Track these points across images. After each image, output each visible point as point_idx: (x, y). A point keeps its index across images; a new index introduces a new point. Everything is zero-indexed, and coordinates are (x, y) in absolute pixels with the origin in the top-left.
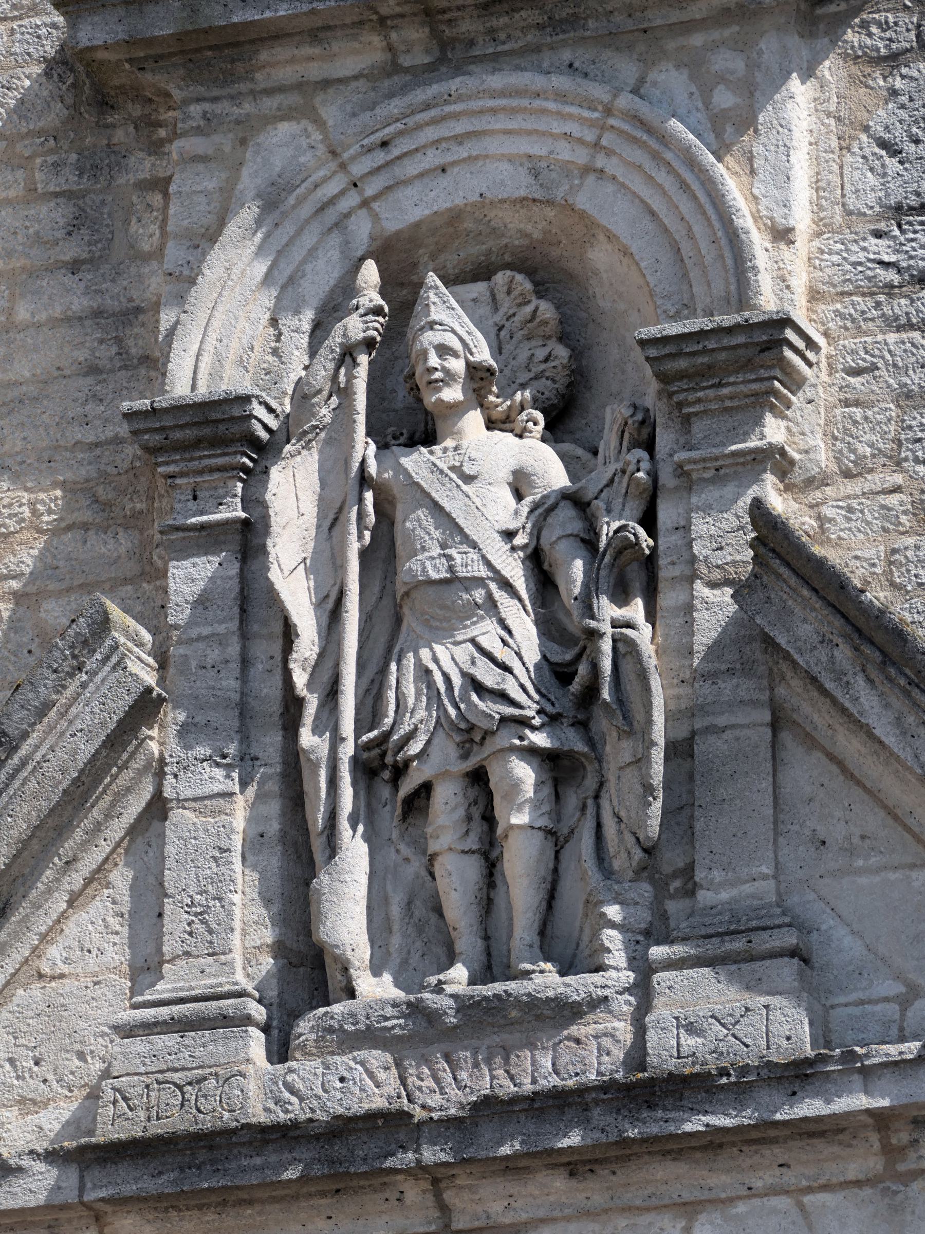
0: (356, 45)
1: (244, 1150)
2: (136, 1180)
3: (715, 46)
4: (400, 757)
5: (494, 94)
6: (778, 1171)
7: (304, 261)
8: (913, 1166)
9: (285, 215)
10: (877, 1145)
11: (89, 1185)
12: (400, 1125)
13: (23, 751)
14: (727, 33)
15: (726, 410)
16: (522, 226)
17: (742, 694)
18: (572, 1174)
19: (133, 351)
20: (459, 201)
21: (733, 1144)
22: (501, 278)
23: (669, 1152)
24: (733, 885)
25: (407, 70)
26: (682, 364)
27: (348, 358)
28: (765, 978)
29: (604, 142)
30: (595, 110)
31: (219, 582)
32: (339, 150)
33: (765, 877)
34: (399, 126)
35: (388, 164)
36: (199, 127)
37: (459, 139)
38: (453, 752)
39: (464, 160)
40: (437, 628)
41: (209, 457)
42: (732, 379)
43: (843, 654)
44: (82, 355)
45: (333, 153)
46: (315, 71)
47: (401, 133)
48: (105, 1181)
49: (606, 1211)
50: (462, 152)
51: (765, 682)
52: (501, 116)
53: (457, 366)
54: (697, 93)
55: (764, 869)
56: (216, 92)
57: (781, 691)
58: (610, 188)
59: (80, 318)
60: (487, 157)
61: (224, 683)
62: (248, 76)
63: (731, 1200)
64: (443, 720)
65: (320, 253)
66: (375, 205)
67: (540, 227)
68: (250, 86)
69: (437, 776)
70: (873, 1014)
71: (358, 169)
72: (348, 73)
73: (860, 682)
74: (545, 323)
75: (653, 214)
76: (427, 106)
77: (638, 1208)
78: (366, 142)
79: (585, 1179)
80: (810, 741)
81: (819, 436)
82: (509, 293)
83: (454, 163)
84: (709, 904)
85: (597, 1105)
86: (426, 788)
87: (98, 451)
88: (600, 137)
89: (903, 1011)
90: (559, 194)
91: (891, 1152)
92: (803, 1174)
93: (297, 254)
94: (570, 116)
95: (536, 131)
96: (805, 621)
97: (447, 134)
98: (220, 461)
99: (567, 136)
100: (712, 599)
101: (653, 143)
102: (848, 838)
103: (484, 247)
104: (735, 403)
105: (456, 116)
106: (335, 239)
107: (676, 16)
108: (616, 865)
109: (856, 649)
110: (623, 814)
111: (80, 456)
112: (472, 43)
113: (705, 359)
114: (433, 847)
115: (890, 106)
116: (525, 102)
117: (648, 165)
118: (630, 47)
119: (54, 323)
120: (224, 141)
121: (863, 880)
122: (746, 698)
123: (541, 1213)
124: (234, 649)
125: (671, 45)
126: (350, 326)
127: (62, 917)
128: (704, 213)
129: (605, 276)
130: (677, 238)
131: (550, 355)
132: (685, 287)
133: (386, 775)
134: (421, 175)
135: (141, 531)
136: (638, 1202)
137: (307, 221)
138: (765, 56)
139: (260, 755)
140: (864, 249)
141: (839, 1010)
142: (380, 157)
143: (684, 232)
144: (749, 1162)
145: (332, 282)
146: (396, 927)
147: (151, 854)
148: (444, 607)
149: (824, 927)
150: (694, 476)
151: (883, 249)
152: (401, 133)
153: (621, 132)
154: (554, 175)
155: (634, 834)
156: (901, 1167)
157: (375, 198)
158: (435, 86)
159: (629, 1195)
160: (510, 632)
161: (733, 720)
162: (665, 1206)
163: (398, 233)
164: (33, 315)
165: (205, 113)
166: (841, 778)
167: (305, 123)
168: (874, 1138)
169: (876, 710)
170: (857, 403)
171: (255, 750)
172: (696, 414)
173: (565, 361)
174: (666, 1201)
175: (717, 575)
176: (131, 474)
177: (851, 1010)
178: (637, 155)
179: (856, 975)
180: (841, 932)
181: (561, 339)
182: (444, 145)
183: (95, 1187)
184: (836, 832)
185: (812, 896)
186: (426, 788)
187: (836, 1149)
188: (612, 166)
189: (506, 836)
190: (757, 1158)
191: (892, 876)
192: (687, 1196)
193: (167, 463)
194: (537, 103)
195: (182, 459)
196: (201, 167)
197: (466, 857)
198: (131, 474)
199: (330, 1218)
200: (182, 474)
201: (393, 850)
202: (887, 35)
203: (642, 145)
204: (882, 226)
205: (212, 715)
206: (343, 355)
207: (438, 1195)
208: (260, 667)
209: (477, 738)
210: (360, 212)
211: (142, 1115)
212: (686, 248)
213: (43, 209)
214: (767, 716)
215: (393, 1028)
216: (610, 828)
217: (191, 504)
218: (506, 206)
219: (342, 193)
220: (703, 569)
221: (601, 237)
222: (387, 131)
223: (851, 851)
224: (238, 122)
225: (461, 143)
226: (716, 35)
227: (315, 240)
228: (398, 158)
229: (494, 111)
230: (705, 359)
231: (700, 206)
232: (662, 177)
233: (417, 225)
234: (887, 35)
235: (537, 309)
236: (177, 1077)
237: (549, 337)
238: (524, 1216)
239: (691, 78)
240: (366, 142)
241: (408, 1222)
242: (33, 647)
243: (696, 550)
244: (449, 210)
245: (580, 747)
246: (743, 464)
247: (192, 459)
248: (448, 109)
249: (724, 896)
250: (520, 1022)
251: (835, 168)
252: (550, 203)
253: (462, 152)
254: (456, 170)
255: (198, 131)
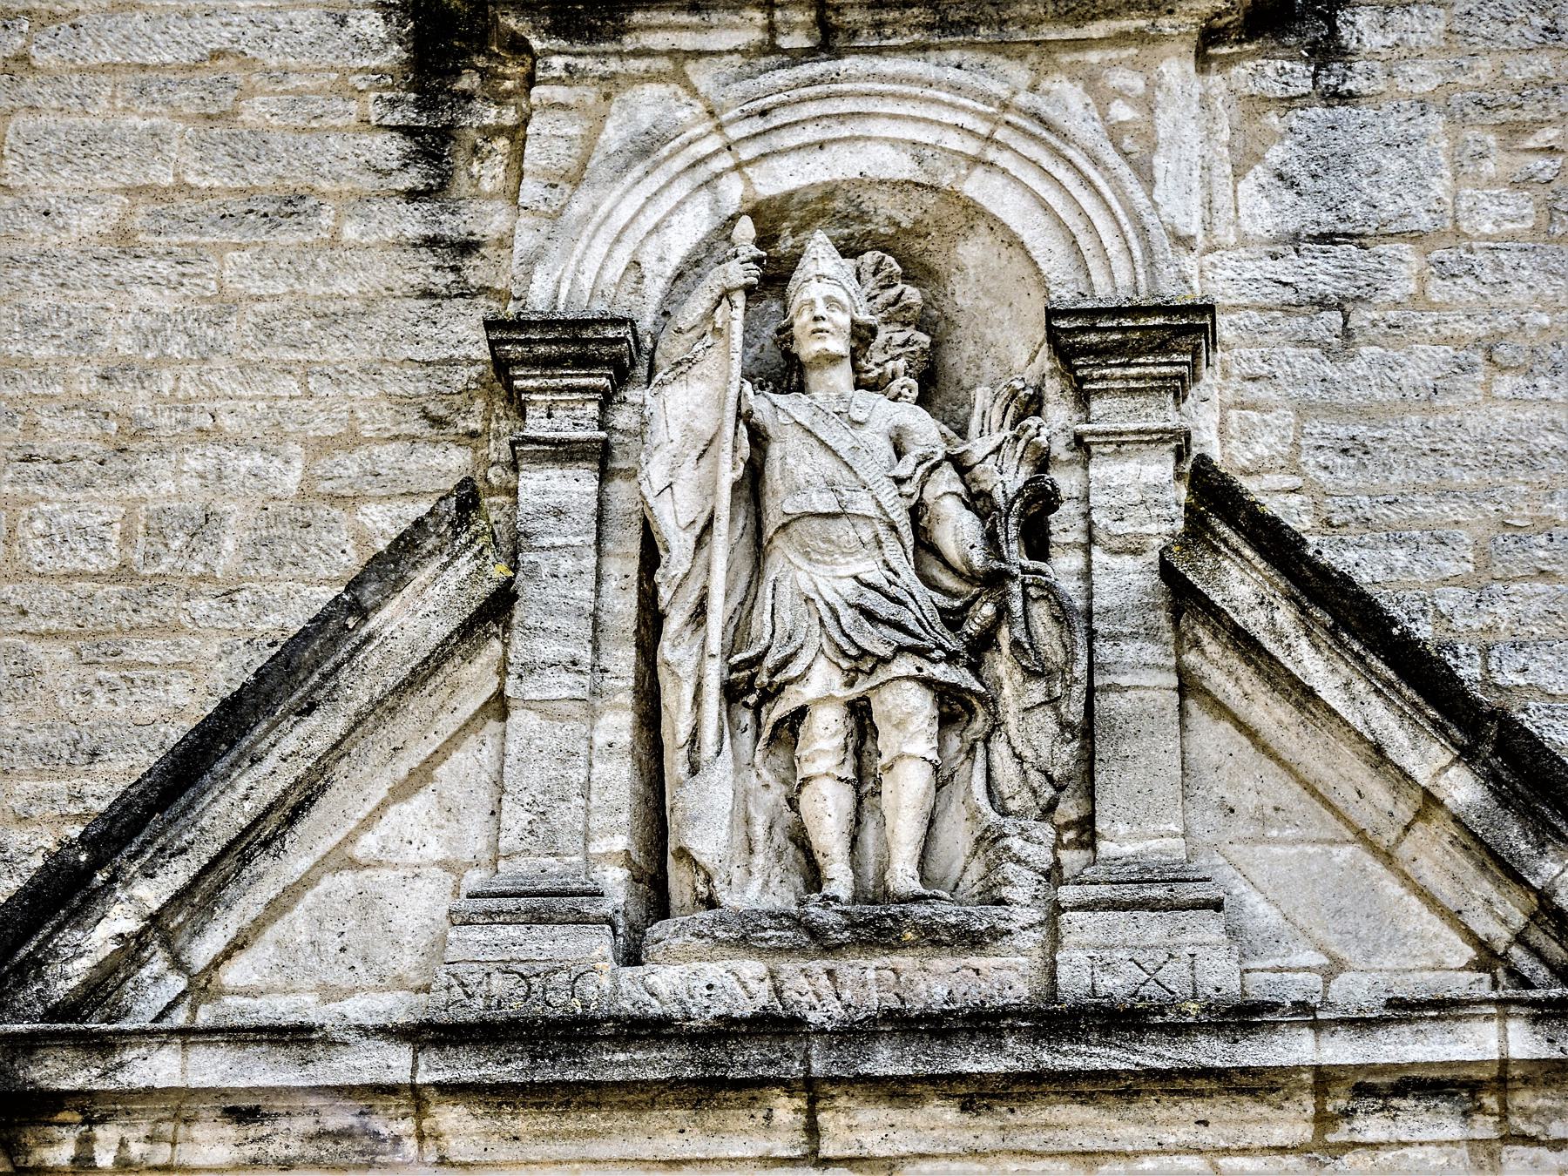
0: (736, 19)
1: (606, 1045)
2: (479, 1066)
3: (1112, 64)
4: (778, 679)
5: (883, 78)
6: (1193, 1128)
7: (671, 213)
8: (1345, 1138)
9: (657, 165)
10: (1311, 1111)
11: (423, 1067)
12: (788, 1034)
13: (373, 624)
14: (1125, 54)
15: (1130, 391)
16: (893, 213)
17: (1146, 657)
18: (964, 1109)
19: (472, 281)
20: (838, 176)
21: (1153, 1093)
22: (870, 258)
23: (1079, 1094)
24: (1138, 839)
25: (785, 52)
26: (1094, 338)
27: (724, 301)
28: (1189, 928)
29: (998, 136)
30: (991, 105)
31: (575, 496)
32: (717, 111)
33: (1174, 835)
34: (783, 97)
35: (765, 132)
36: (559, 78)
37: (841, 118)
38: (838, 679)
39: (845, 139)
40: (817, 561)
41: (571, 376)
42: (1141, 360)
43: (1285, 616)
44: (416, 279)
45: (711, 113)
46: (687, 41)
47: (783, 104)
48: (442, 1065)
49: (994, 1153)
50: (844, 131)
51: (1171, 649)
52: (889, 101)
53: (844, 320)
54: (1093, 105)
55: (1172, 827)
56: (579, 48)
57: (1191, 658)
58: (999, 181)
59: (414, 245)
60: (869, 138)
61: (578, 593)
62: (619, 32)
63: (1137, 1154)
64: (825, 647)
65: (688, 206)
66: (748, 170)
67: (912, 215)
68: (616, 46)
69: (818, 701)
70: (1293, 982)
71: (734, 132)
72: (723, 47)
73: (1304, 643)
74: (908, 308)
75: (1046, 208)
76: (813, 82)
77: (1032, 1153)
78: (745, 107)
79: (979, 1114)
80: (1220, 709)
81: (1214, 432)
82: (875, 274)
83: (834, 141)
84: (1113, 855)
85: (1012, 1032)
86: (801, 713)
87: (430, 370)
88: (993, 132)
89: (1327, 983)
90: (945, 181)
91: (1323, 1120)
92: (1221, 1135)
93: (666, 202)
94: (964, 108)
95: (925, 120)
96: (1243, 581)
97: (830, 111)
98: (584, 382)
99: (959, 128)
100: (1112, 564)
101: (1052, 139)
102: (1259, 808)
103: (846, 231)
104: (1141, 385)
105: (841, 95)
106: (704, 196)
107: (1071, 33)
108: (1013, 805)
109: (1303, 610)
110: (1028, 753)
111: (410, 372)
112: (855, 34)
113: (1118, 337)
114: (806, 770)
115: (1287, 142)
116: (916, 90)
117: (1046, 161)
118: (1022, 56)
119: (386, 246)
120: (589, 94)
121: (1277, 850)
122: (1151, 661)
123: (922, 1148)
124: (590, 562)
125: (1065, 58)
126: (730, 270)
127: (383, 805)
128: (1109, 208)
129: (972, 272)
130: (1074, 230)
131: (908, 340)
132: (1082, 277)
133: (752, 699)
134: (799, 148)
135: (475, 449)
136: (1033, 1147)
137: (678, 175)
138: (1167, 78)
139: (611, 668)
140: (1260, 268)
141: (1253, 974)
142: (758, 125)
143: (1082, 226)
144: (1165, 1114)
145: (700, 236)
146: (759, 847)
147: (485, 752)
148: (826, 540)
149: (1235, 892)
150: (1094, 449)
151: (1282, 270)
152: (783, 104)
153: (1017, 128)
154: (939, 163)
155: (1045, 773)
156: (1331, 1138)
157: (749, 163)
158: (823, 64)
159: (1024, 1138)
160: (896, 574)
161: (1136, 681)
162: (1062, 1154)
163: (771, 199)
164: (362, 235)
165: (567, 66)
166: (1252, 750)
167: (674, 87)
168: (1309, 1102)
169: (1321, 674)
170: (1254, 407)
171: (604, 662)
172: (1096, 392)
173: (926, 346)
174: (1065, 1148)
175: (1115, 544)
176: (465, 395)
177: (1267, 975)
178: (1035, 151)
179: (1272, 942)
180: (1253, 900)
181: (918, 328)
182: (825, 122)
183: (429, 1069)
184: (1248, 802)
185: (1221, 861)
186: (801, 713)
187: (1264, 1110)
188: (1004, 159)
189: (891, 767)
190: (1175, 1111)
191: (1310, 850)
192: (1088, 1145)
193: (525, 377)
194: (929, 92)
195: (542, 376)
196: (561, 114)
197: (842, 785)
198: (465, 395)
199: (682, 1131)
200: (540, 390)
201: (754, 774)
202: (1284, 79)
203: (1042, 142)
204: (1279, 249)
205: (563, 622)
206: (721, 297)
207: (811, 1114)
208: (614, 584)
209: (866, 667)
210: (731, 175)
211: (480, 1002)
212: (1084, 241)
213: (380, 139)
214: (1174, 681)
215: (770, 939)
216: (1006, 771)
217: (545, 422)
218: (884, 188)
219: (716, 153)
220: (1103, 537)
221: (982, 228)
222: (769, 99)
223: (1263, 821)
224: (602, 78)
225: (842, 123)
226: (1113, 54)
227: (685, 193)
228: (776, 128)
229: (881, 95)
230: (1118, 337)
231: (1104, 201)
232: (1060, 172)
233: (790, 195)
234: (1284, 79)
235: (902, 292)
236: (521, 968)
237: (909, 324)
238: (903, 1150)
239: (1086, 90)
240: (745, 107)
241: (769, 1145)
242: (348, 548)
243: (1094, 517)
244: (826, 184)
245: (977, 687)
246: (1148, 442)
247: (552, 377)
248: (834, 87)
249: (1129, 849)
250: (913, 945)
251: (1230, 192)
252: (934, 189)
253: (844, 131)
254: (834, 147)
255: (559, 81)
